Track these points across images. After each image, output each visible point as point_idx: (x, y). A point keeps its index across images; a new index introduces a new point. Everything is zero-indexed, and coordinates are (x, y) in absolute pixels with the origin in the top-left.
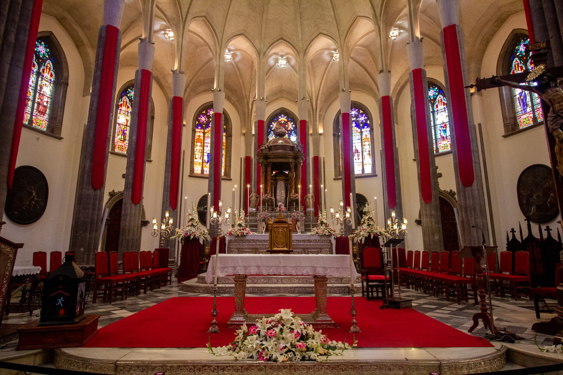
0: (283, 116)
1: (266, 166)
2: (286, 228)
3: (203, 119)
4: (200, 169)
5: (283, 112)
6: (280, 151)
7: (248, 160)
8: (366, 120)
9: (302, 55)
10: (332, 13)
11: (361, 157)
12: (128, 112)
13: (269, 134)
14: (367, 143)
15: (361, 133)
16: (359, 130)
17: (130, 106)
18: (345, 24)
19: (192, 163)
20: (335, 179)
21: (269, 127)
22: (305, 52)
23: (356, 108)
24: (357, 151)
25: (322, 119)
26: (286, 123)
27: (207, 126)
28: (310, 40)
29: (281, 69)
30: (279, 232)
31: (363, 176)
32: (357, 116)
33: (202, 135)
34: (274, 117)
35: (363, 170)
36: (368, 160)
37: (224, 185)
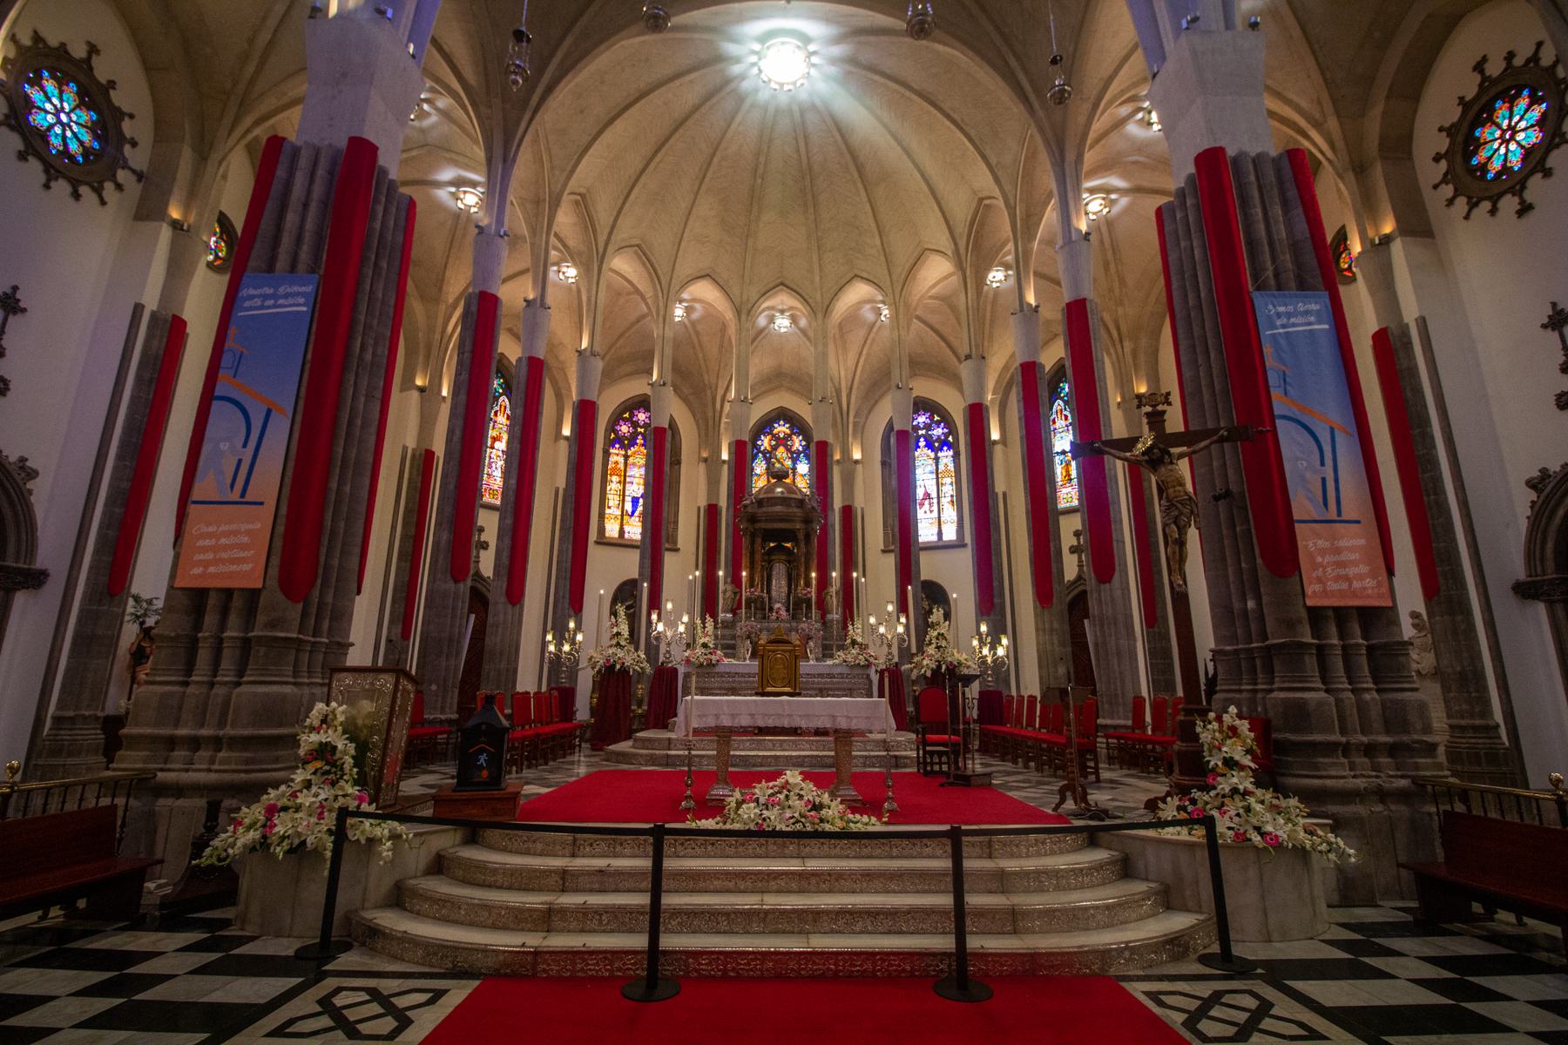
1: (753, 535)
3: (624, 429)
4: (617, 528)
6: (778, 508)
7: (712, 511)
8: (946, 435)
9: (820, 316)
10: (878, 242)
11: (935, 508)
13: (754, 457)
14: (948, 480)
15: (937, 459)
16: (932, 455)
18: (902, 260)
19: (602, 516)
20: (884, 551)
21: (755, 446)
22: (827, 311)
23: (926, 411)
24: (927, 496)
25: (860, 430)
26: (788, 437)
27: (633, 443)
28: (836, 288)
29: (781, 335)
31: (940, 546)
32: (928, 427)
33: (621, 460)
34: (765, 426)
35: (940, 533)
36: (950, 514)
37: (669, 560)
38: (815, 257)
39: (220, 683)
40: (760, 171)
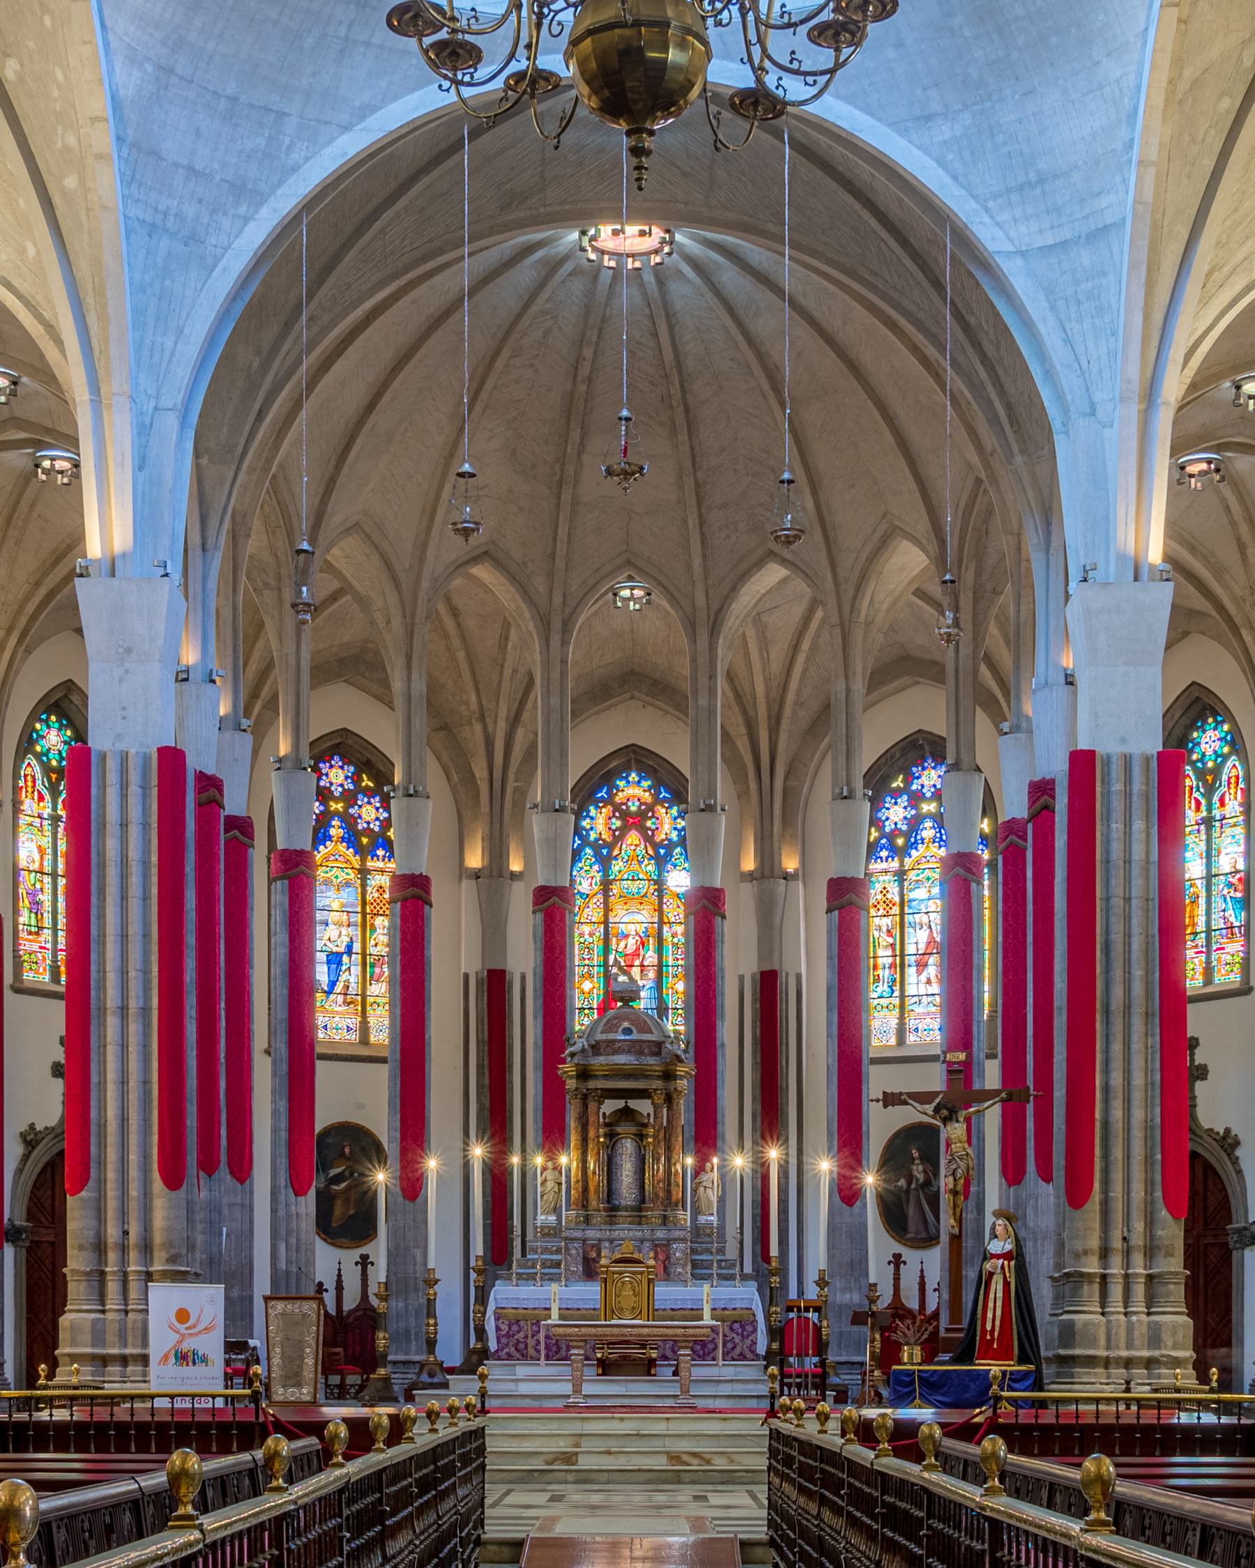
0: (634, 777)
1: (585, 1098)
2: (641, 1273)
5: (637, 758)
9: (703, 635)
12: (40, 816)
13: (577, 855)
17: (45, 792)
30: (623, 1283)
38: (693, 521)
39: (133, 1310)
40: (585, 370)
